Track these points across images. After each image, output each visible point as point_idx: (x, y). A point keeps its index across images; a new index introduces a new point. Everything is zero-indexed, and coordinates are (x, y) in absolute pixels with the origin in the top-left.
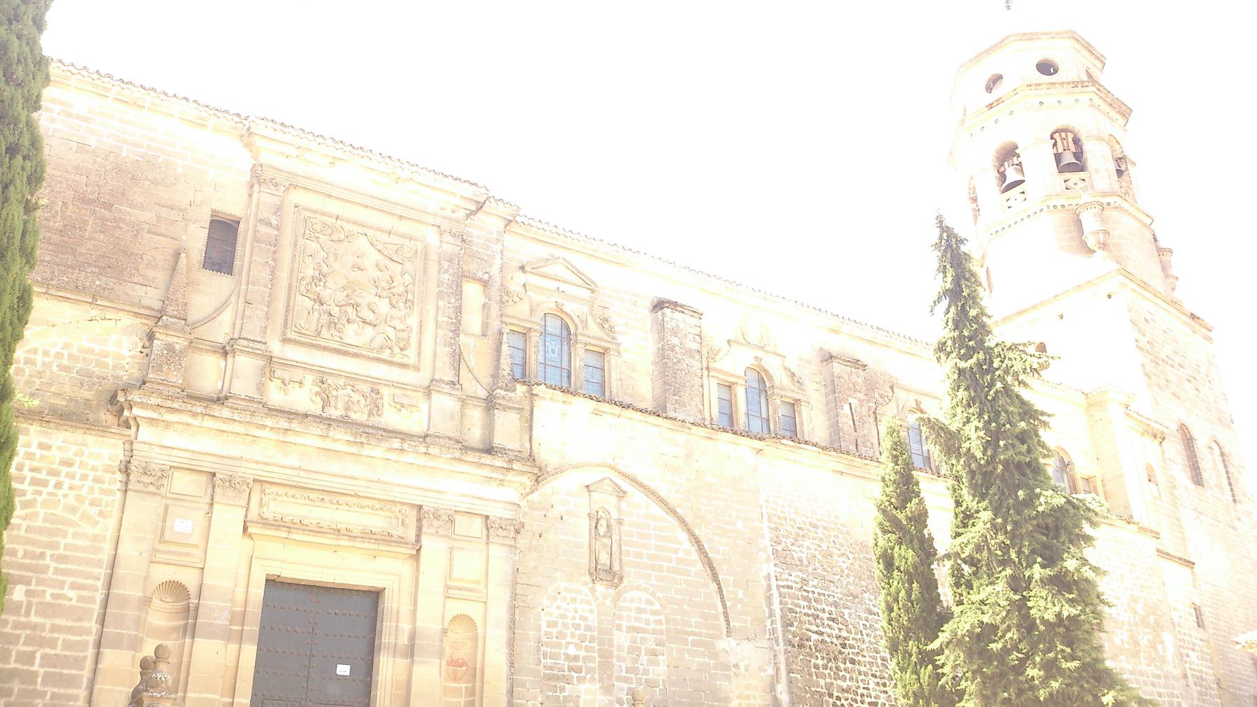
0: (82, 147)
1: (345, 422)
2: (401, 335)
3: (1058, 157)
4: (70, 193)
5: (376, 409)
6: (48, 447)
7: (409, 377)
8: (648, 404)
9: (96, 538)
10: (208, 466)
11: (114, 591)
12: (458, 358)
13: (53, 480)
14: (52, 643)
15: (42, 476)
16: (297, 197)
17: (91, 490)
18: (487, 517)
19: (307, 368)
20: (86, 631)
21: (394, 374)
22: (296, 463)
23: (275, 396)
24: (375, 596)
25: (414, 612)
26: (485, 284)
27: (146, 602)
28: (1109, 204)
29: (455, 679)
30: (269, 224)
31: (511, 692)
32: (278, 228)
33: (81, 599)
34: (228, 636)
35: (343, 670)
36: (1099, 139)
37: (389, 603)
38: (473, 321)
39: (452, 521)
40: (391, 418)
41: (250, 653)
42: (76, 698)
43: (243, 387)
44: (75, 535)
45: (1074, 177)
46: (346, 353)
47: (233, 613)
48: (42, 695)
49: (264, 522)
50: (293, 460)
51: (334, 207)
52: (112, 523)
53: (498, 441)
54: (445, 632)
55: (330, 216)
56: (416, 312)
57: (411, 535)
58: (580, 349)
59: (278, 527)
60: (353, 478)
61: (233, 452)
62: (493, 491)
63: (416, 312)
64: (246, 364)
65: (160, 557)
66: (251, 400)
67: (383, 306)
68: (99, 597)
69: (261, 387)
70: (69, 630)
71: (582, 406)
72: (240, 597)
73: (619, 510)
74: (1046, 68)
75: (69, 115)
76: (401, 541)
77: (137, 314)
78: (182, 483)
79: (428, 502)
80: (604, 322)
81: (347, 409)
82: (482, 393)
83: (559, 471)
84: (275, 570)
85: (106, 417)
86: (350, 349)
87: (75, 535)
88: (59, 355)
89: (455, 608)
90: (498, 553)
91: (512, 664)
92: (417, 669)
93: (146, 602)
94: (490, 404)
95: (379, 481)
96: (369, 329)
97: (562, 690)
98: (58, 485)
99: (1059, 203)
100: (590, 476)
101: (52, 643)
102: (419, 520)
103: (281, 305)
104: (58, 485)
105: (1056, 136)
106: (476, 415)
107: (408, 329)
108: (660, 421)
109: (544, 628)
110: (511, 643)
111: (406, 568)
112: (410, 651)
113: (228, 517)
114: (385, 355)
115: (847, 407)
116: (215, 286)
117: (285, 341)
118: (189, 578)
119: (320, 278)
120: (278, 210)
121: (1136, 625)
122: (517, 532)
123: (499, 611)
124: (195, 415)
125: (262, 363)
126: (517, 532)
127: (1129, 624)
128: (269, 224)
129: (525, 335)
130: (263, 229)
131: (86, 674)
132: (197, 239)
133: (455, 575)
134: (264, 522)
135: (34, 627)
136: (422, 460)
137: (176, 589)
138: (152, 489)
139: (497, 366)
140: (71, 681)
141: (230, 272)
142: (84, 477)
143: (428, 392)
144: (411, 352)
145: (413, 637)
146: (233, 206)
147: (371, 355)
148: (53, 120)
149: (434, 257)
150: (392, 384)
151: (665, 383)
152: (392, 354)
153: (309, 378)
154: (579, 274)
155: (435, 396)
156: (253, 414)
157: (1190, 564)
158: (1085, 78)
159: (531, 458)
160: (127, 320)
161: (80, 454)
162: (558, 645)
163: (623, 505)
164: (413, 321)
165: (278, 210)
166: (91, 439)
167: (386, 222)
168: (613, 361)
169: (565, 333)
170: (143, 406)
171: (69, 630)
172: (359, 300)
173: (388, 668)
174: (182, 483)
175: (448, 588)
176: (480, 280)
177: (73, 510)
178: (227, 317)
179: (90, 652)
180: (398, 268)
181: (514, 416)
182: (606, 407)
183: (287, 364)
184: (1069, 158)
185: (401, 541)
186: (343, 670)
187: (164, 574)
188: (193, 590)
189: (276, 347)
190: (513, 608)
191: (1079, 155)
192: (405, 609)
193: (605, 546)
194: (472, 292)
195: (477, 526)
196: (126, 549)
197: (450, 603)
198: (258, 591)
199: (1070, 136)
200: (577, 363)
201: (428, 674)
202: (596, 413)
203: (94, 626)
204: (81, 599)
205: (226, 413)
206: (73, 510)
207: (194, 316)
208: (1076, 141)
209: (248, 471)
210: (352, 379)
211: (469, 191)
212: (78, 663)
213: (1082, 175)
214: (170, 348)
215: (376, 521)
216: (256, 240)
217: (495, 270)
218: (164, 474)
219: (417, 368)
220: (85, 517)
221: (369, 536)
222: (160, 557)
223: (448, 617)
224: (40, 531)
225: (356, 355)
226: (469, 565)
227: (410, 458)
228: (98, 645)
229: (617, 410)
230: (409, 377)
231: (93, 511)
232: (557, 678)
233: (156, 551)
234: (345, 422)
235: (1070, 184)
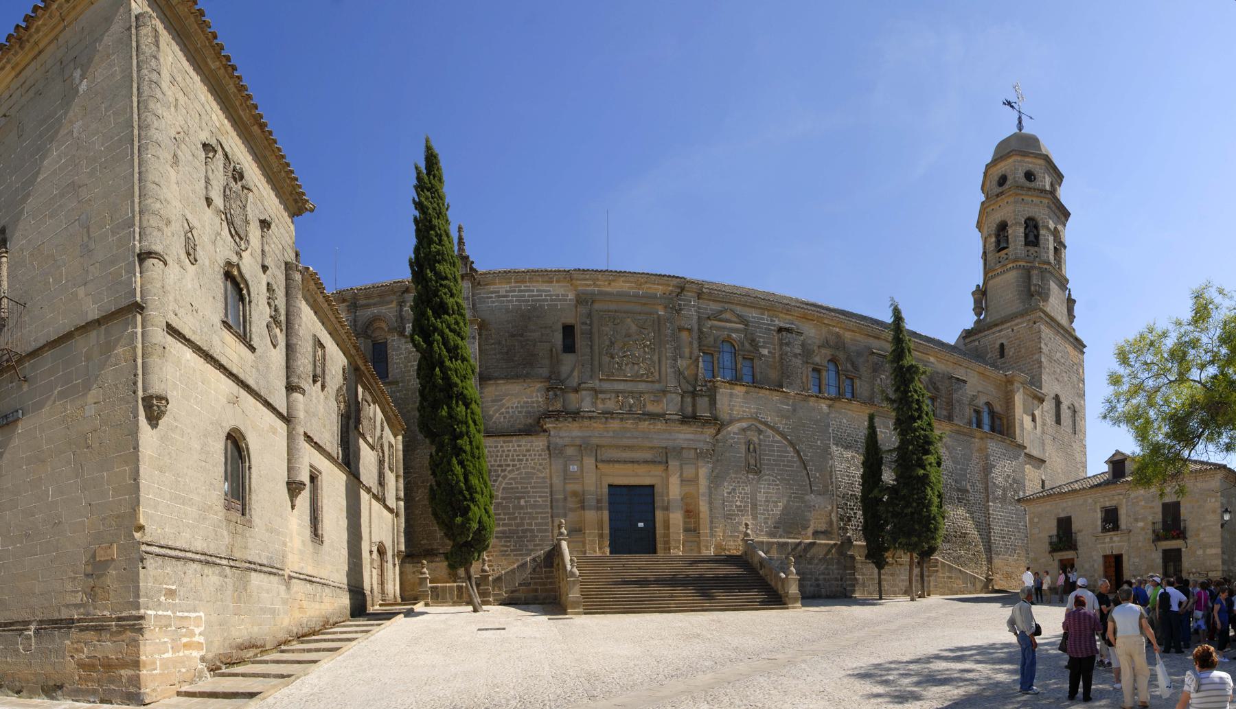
10: (578, 442)
14: (537, 518)
20: (547, 512)
42: (548, 536)
61: (588, 435)
78: (570, 451)
87: (537, 478)
113: (589, 462)
115: (879, 380)
124: (569, 422)
140: (546, 531)
159: (716, 419)
169: (733, 351)
178: (575, 373)
183: (602, 392)
193: (752, 457)
207: (563, 376)
212: (547, 524)
220: (539, 470)
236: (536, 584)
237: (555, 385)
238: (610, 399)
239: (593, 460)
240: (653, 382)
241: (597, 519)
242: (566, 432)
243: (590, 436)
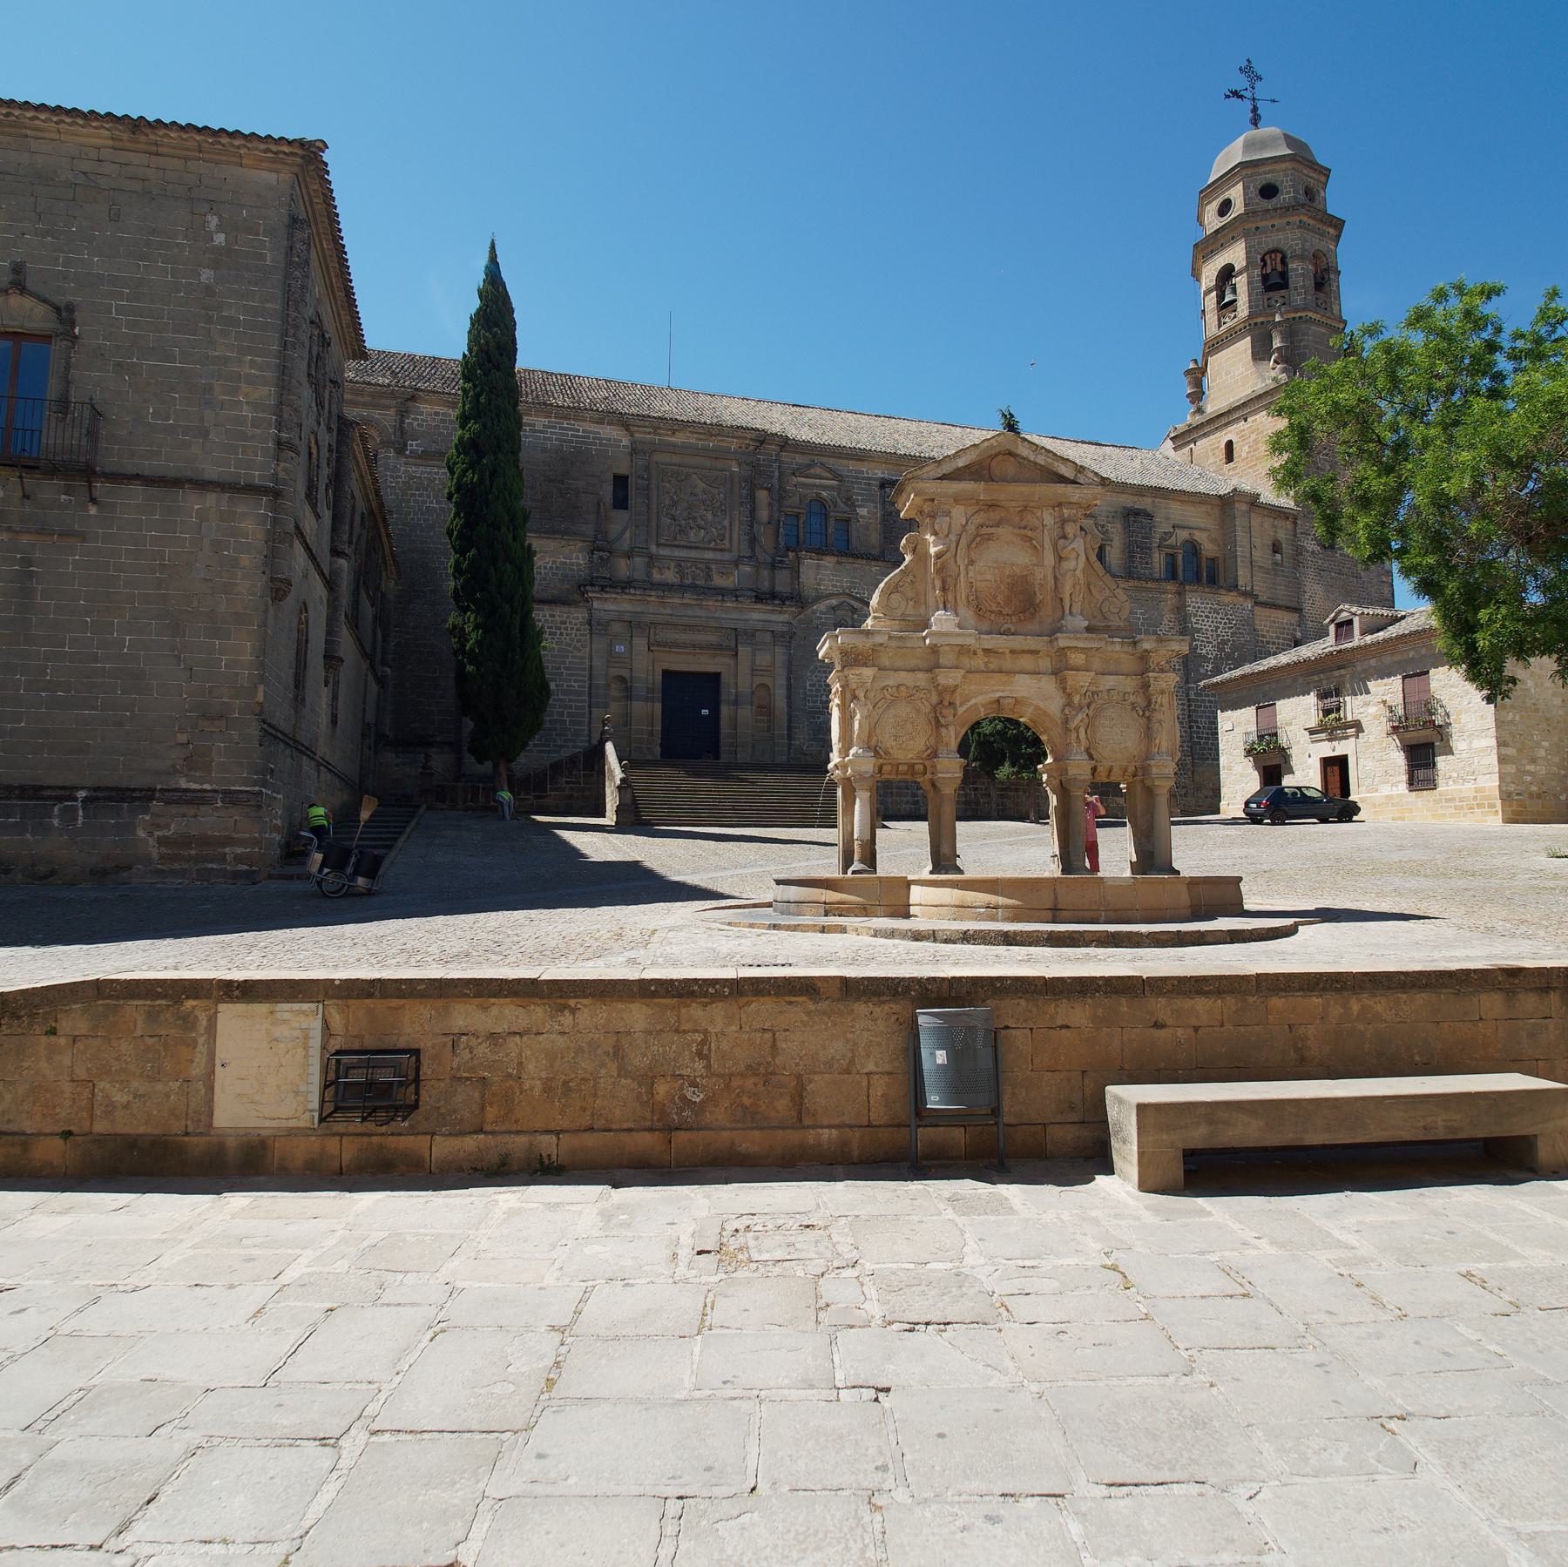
0: (544, 450)
1: (693, 588)
2: (720, 532)
3: (1265, 278)
4: (543, 478)
5: (709, 577)
6: (553, 616)
7: (727, 556)
8: (876, 552)
9: (581, 658)
10: (627, 617)
11: (594, 682)
12: (753, 541)
13: (558, 632)
14: (571, 707)
15: (554, 630)
16: (658, 457)
17: (576, 635)
18: (773, 632)
19: (671, 558)
21: (718, 556)
22: (671, 612)
23: (656, 576)
24: (717, 676)
25: (736, 684)
26: (769, 490)
27: (608, 686)
28: (1300, 318)
29: (762, 715)
30: (643, 478)
31: (789, 721)
32: (648, 479)
33: (579, 686)
34: (647, 699)
35: (705, 712)
36: (1301, 258)
37: (724, 679)
38: (763, 514)
39: (753, 635)
40: (719, 581)
41: (658, 706)
42: (583, 730)
43: (639, 575)
44: (572, 657)
45: (1276, 295)
46: (690, 547)
47: (648, 689)
48: (570, 730)
49: (659, 644)
50: (668, 611)
51: (676, 459)
52: (588, 650)
53: (778, 588)
54: (753, 693)
55: (675, 465)
56: (728, 517)
57: (733, 645)
58: (832, 521)
59: (665, 646)
60: (700, 617)
61: (639, 609)
62: (774, 617)
63: (728, 517)
64: (639, 561)
65: (612, 664)
66: (645, 581)
67: (709, 516)
68: (587, 685)
69: (649, 574)
70: (576, 701)
71: (829, 561)
72: (651, 681)
73: (853, 619)
74: (1269, 191)
75: (535, 431)
76: (728, 648)
77: (584, 541)
78: (616, 628)
79: (740, 626)
80: (849, 501)
81: (694, 579)
82: (769, 560)
83: (818, 599)
84: (666, 666)
85: (577, 597)
86: (693, 545)
88: (551, 568)
89: (758, 680)
90: (778, 650)
91: (789, 706)
92: (739, 711)
93: (608, 686)
94: (773, 567)
95: (713, 617)
96: (702, 531)
97: (819, 718)
98: (561, 634)
99: (1259, 320)
100: (834, 602)
101: (571, 707)
102: (736, 636)
103: (654, 524)
104: (561, 634)
105: (1267, 257)
106: (766, 573)
107: (724, 527)
108: (880, 563)
109: (808, 688)
110: (789, 697)
111: (732, 662)
112: (736, 703)
113: (640, 643)
114: (712, 546)
116: (622, 516)
117: (658, 545)
118: (625, 673)
119: (674, 504)
120: (647, 468)
121: (1221, 658)
122: (791, 638)
123: (781, 681)
125: (647, 560)
126: (791, 638)
127: (1215, 658)
128: (643, 478)
129: (797, 516)
130: (640, 481)
131: (587, 720)
132: (607, 491)
133: (757, 663)
134: (659, 644)
135: (562, 700)
136: (734, 605)
137: (622, 679)
138: (603, 632)
139: (777, 543)
141: (627, 509)
142: (572, 629)
143: (736, 563)
144: (726, 541)
145: (737, 696)
146: (623, 471)
147: (706, 546)
148: (527, 437)
149: (737, 480)
150: (716, 562)
151: (885, 538)
152: (716, 544)
153: (673, 564)
154: (830, 470)
155: (740, 567)
156: (645, 589)
157: (1298, 610)
158: (1302, 197)
160: (580, 544)
161: (568, 617)
162: (817, 696)
163: (855, 616)
164: (726, 523)
165: (647, 468)
166: (572, 609)
167: (707, 463)
168: (853, 526)
170: (593, 592)
171: (576, 701)
172: (695, 515)
173: (725, 711)
174: (616, 628)
175: (753, 670)
176: (766, 489)
177: (570, 645)
178: (627, 534)
179: (587, 709)
180: (716, 491)
181: (786, 573)
182: (844, 559)
184: (1275, 279)
185: (728, 648)
186: (705, 712)
187: (614, 672)
188: (628, 679)
189: (653, 549)
190: (789, 679)
191: (1284, 275)
192: (732, 681)
194: (762, 496)
195: (768, 637)
196: (596, 662)
197: (755, 678)
198: (659, 678)
199: (1279, 255)
200: (831, 530)
201: (745, 713)
202: (839, 563)
203: (587, 698)
204: (579, 686)
205: (632, 591)
206: (570, 645)
208: (1283, 261)
209: (648, 618)
210: (695, 561)
211: (753, 435)
213: (1282, 292)
214: (601, 558)
215: (712, 638)
216: (637, 489)
217: (775, 481)
218: (609, 622)
219: (730, 550)
221: (710, 646)
222: (612, 664)
223: (755, 686)
224: (556, 656)
225: (696, 548)
226: (763, 659)
227: (729, 605)
228: (590, 707)
229: (851, 560)
230: (727, 556)
231: (579, 645)
232: (816, 712)
233: (609, 662)
234: (693, 588)
235: (1273, 302)
236: (572, 789)
237: (601, 547)
238: (669, 569)
239: (645, 641)
240: (721, 550)
241: (648, 712)
242: (610, 605)
243: (642, 613)
